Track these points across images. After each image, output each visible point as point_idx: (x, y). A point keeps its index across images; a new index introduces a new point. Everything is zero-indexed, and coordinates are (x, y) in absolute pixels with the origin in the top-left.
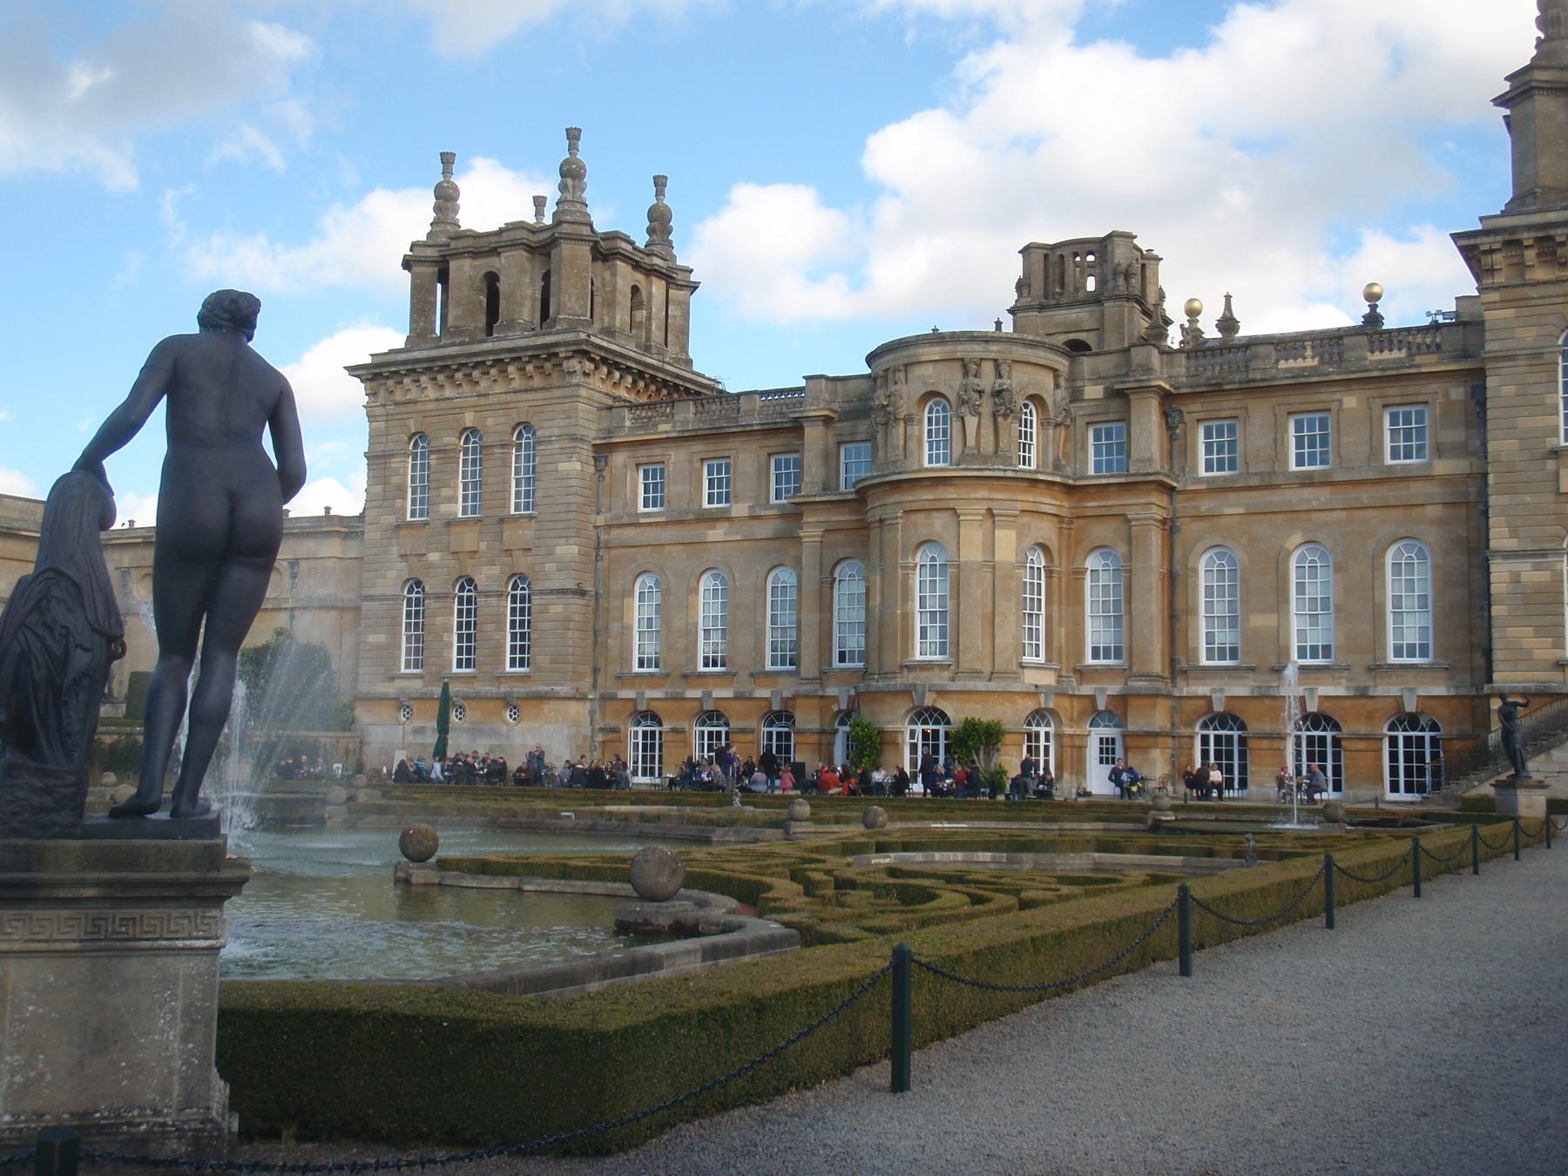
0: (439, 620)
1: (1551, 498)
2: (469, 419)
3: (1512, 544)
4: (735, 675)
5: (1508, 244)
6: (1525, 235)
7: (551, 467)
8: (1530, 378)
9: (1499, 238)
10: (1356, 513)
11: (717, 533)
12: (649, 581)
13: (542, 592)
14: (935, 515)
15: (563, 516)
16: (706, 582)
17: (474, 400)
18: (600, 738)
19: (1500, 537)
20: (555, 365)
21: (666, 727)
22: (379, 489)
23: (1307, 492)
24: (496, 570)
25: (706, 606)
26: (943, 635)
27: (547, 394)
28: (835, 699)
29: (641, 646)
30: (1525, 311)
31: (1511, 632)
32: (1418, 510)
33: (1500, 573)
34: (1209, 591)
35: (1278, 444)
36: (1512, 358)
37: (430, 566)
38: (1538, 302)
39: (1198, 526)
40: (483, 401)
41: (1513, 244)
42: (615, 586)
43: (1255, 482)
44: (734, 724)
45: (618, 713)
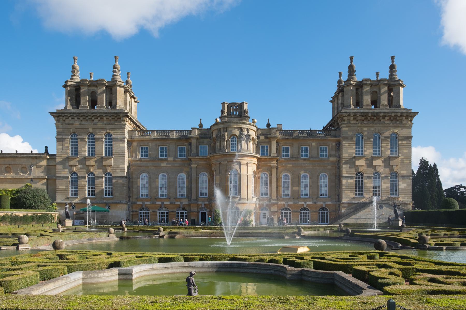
0: (83, 183)
3: (347, 175)
4: (170, 198)
7: (117, 145)
8: (350, 142)
11: (164, 164)
12: (144, 175)
16: (160, 176)
17: (92, 125)
18: (131, 214)
19: (344, 173)
20: (118, 118)
21: (151, 211)
22: (61, 147)
25: (161, 181)
28: (201, 205)
29: (143, 191)
31: (346, 192)
34: (284, 182)
35: (299, 151)
40: (95, 126)
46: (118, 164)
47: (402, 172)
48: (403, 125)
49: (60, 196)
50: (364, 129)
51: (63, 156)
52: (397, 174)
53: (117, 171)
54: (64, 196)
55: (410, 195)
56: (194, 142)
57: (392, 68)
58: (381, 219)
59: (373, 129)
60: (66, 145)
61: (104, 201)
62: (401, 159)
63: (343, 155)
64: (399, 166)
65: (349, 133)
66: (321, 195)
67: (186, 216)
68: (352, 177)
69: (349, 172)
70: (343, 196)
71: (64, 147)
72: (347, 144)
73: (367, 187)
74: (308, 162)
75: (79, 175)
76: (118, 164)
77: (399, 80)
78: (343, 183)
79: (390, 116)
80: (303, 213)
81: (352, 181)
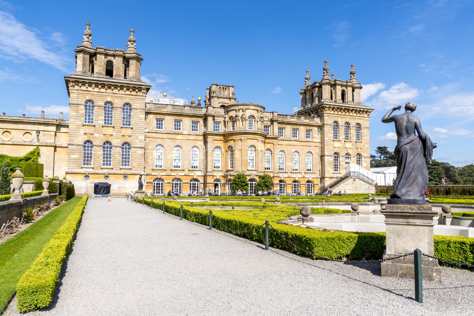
0: (98, 152)
2: (109, 99)
11: (179, 137)
13: (135, 147)
15: (141, 129)
19: (326, 153)
22: (75, 113)
24: (119, 140)
26: (253, 164)
27: (136, 97)
33: (326, 158)
37: (95, 137)
39: (279, 146)
42: (150, 147)
43: (288, 139)
44: (184, 181)
45: (151, 178)
46: (137, 135)
47: (364, 154)
49: (72, 165)
51: (76, 122)
53: (136, 141)
54: (77, 165)
56: (210, 119)
60: (80, 112)
61: (122, 172)
67: (197, 187)
68: (331, 156)
71: (78, 114)
72: (327, 130)
75: (94, 144)
76: (137, 135)
78: (326, 161)
79: (356, 111)
81: (331, 159)
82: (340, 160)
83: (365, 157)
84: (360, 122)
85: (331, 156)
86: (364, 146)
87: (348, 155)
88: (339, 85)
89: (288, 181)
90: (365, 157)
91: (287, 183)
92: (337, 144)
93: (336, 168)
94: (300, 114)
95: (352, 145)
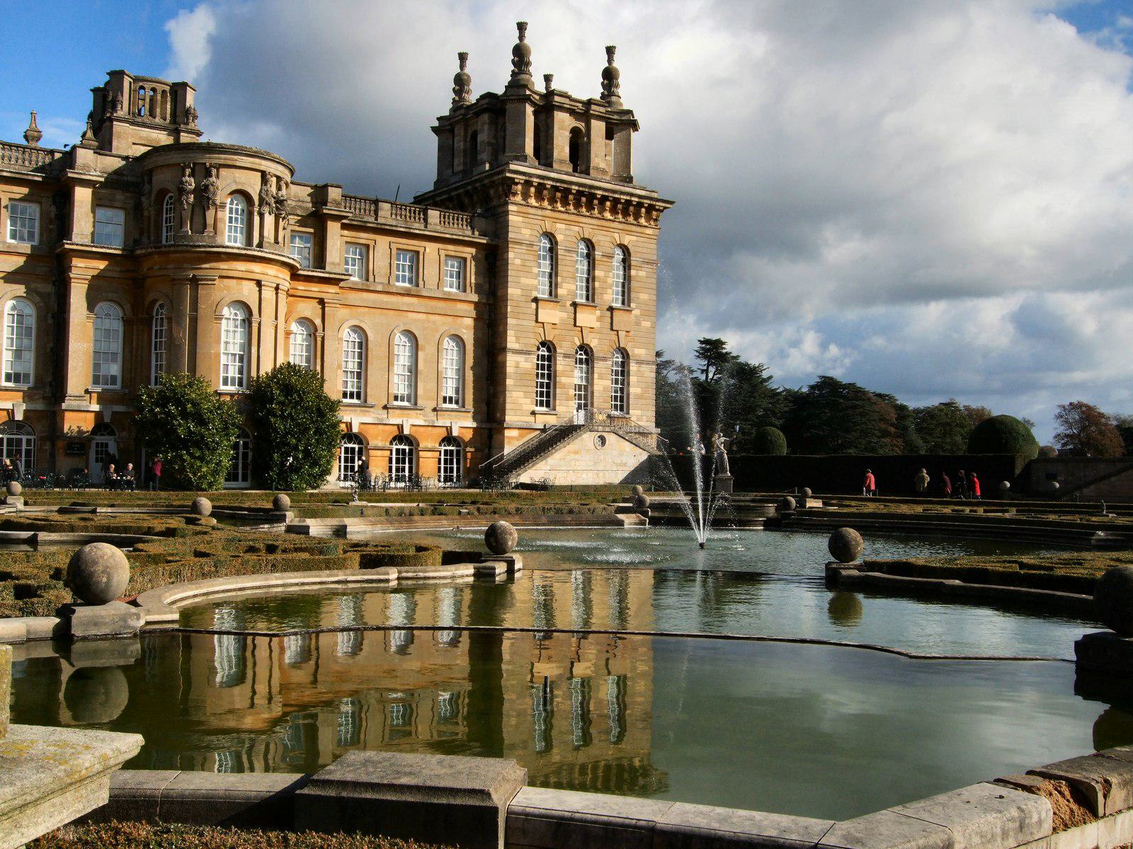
1: (533, 323)
5: (526, 182)
6: (535, 180)
9: (524, 178)
10: (430, 316)
14: (244, 282)
19: (512, 342)
23: (407, 299)
30: (527, 220)
31: (515, 394)
32: (460, 319)
36: (521, 244)
38: (532, 216)
39: (343, 312)
41: (528, 184)
43: (379, 288)
48: (639, 229)
50: (559, 226)
52: (625, 354)
55: (651, 413)
57: (609, 76)
58: (601, 474)
59: (577, 229)
62: (636, 317)
63: (510, 291)
64: (631, 334)
65: (524, 231)
66: (445, 401)
67: (28, 452)
69: (522, 340)
70: (508, 406)
72: (518, 262)
73: (564, 386)
74: (415, 300)
77: (630, 112)
80: (398, 450)
82: (559, 368)
83: (640, 362)
84: (627, 240)
85: (528, 353)
86: (638, 324)
87: (587, 355)
88: (561, 108)
89: (376, 437)
90: (640, 362)
91: (372, 443)
92: (550, 314)
93: (547, 396)
94: (423, 202)
95: (600, 319)
